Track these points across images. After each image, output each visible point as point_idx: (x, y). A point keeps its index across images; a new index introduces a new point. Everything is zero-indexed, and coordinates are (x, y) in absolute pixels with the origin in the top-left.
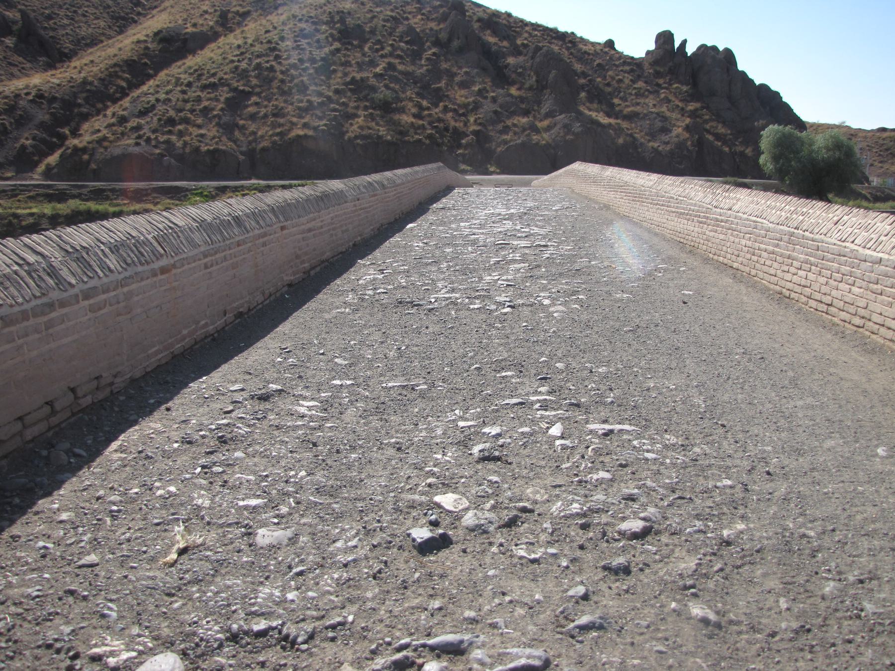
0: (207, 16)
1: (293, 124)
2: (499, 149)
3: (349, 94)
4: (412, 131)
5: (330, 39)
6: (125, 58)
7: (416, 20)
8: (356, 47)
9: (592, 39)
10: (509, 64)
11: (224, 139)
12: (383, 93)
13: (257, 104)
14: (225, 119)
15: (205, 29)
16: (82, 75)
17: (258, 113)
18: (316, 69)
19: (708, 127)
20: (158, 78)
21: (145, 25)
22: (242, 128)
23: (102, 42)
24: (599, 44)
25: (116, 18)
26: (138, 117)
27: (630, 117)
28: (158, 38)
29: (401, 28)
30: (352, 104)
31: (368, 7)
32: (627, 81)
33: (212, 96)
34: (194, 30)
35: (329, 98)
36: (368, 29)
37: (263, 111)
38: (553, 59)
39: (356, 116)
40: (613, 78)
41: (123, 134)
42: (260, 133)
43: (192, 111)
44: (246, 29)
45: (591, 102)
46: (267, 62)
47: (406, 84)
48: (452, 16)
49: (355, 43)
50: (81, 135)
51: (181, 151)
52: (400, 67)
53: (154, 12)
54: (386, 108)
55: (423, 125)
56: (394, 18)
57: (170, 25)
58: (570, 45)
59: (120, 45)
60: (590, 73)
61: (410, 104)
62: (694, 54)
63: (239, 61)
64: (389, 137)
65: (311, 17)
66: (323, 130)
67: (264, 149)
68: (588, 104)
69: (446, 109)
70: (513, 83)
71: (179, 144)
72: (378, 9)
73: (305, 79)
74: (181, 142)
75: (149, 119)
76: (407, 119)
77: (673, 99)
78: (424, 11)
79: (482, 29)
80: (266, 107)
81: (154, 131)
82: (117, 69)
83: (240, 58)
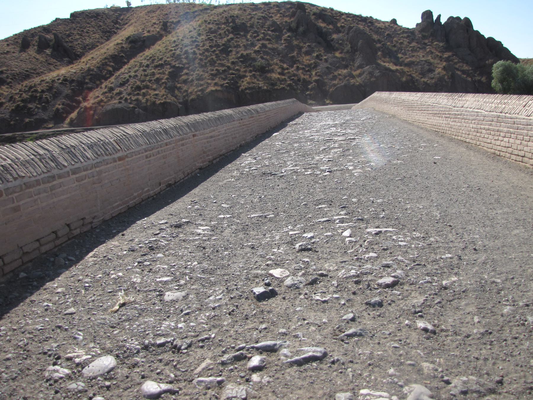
0: (155, 26)
1: (209, 84)
2: (331, 90)
3: (240, 64)
4: (278, 83)
5: (227, 33)
6: (111, 54)
7: (277, 17)
8: (242, 36)
9: (383, 20)
10: (334, 39)
11: (169, 96)
12: (260, 62)
13: (187, 74)
14: (169, 84)
15: (154, 33)
16: (88, 66)
17: (188, 79)
18: (220, 51)
19: (457, 66)
20: (129, 64)
22: (179, 89)
23: (98, 46)
24: (387, 22)
25: (104, 32)
26: (119, 87)
27: (410, 65)
29: (268, 23)
30: (242, 70)
31: (248, 12)
32: (405, 43)
33: (161, 71)
34: (149, 34)
35: (229, 67)
36: (248, 25)
38: (360, 33)
40: (397, 42)
41: (112, 97)
42: (190, 91)
43: (150, 81)
44: (178, 31)
45: (385, 57)
46: (192, 49)
47: (273, 55)
48: (298, 13)
49: (242, 33)
50: (88, 100)
51: (145, 105)
52: (269, 46)
53: (126, 26)
54: (263, 70)
55: (285, 79)
56: (264, 17)
57: (134, 33)
58: (370, 24)
59: (108, 47)
60: (383, 40)
61: (277, 67)
62: (445, 23)
63: (175, 50)
64: (265, 88)
65: (215, 21)
66: (226, 86)
67: (193, 100)
68: (383, 59)
69: (298, 68)
70: (337, 50)
71: (144, 101)
72: (254, 13)
73: (214, 57)
74: (145, 99)
75: (126, 88)
76: (275, 76)
77: (435, 51)
78: (281, 12)
79: (317, 19)
80: (192, 75)
81: (129, 94)
82: (107, 61)
83: (176, 48)
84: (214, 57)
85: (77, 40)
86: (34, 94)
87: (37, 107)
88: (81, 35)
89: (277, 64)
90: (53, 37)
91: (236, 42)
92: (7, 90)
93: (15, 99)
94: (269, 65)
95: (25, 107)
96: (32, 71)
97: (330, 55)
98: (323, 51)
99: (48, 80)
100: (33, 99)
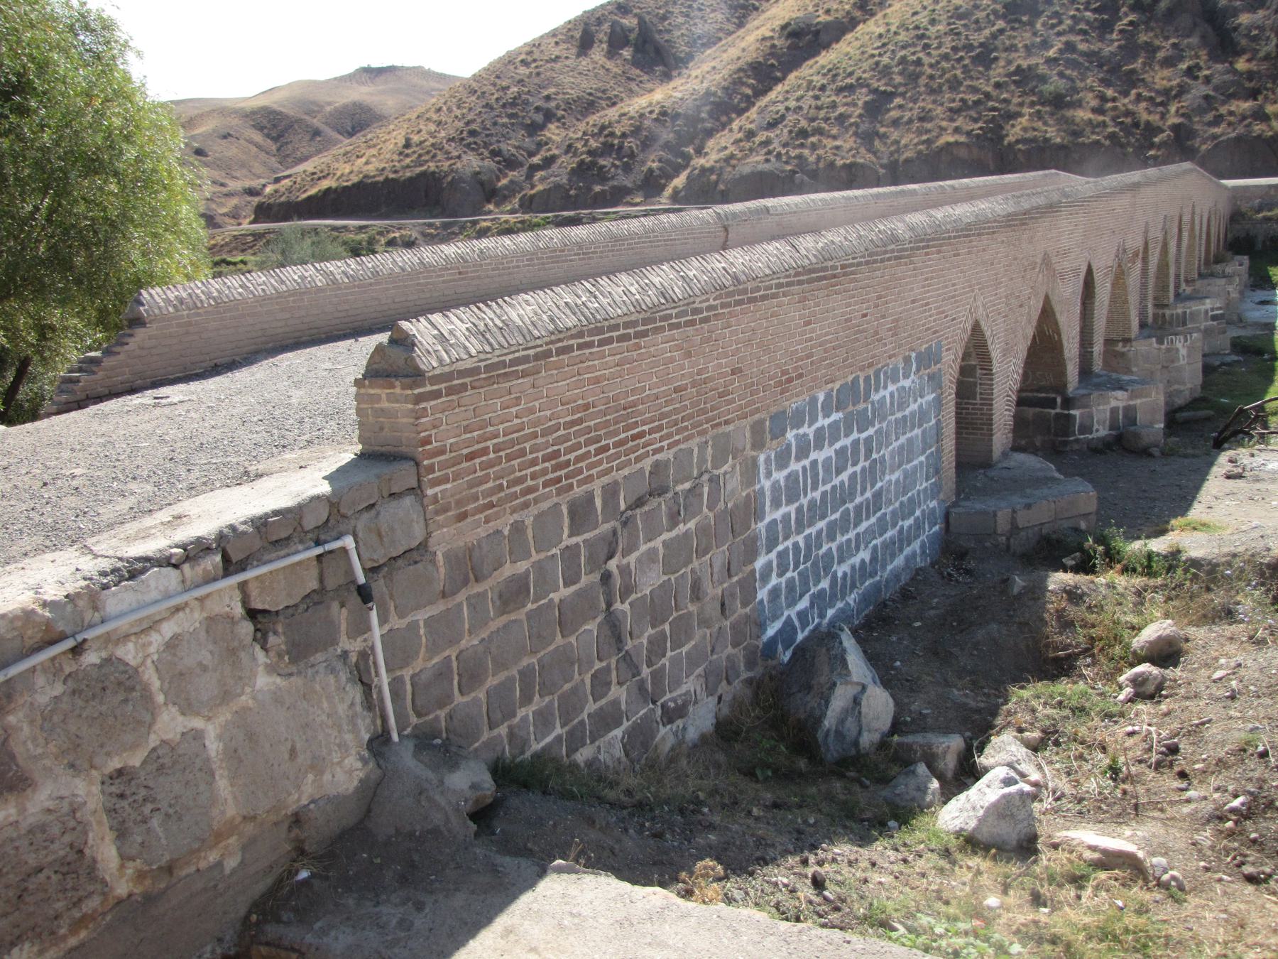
1: (942, 129)
2: (1204, 147)
3: (1013, 87)
4: (1088, 130)
5: (992, 17)
6: (750, 60)
8: (1025, 24)
11: (862, 150)
12: (1056, 83)
13: (900, 107)
14: (863, 127)
15: (839, 15)
16: (705, 85)
17: (902, 117)
20: (786, 82)
21: (768, 14)
22: (883, 137)
23: (720, 39)
28: (786, 32)
30: (1016, 100)
33: (849, 100)
34: (829, 18)
35: (988, 96)
37: (908, 115)
39: (1019, 115)
41: (751, 150)
42: (903, 142)
43: (826, 119)
44: (888, 11)
46: (914, 54)
47: (1087, 68)
49: (1025, 19)
50: (706, 154)
52: (1083, 47)
54: (1058, 102)
55: (1104, 122)
57: (798, 14)
59: (743, 45)
61: (1091, 95)
63: (880, 55)
64: (1058, 140)
66: (978, 136)
67: (907, 161)
70: (1238, 53)
71: (812, 159)
73: (958, 72)
76: (1082, 115)
80: (911, 109)
81: (785, 145)
84: (958, 72)
85: (678, 27)
86: (610, 139)
87: (614, 165)
88: (687, 16)
89: (1091, 89)
90: (635, 21)
91: (1010, 37)
92: (557, 131)
93: (576, 149)
94: (1075, 90)
95: (594, 164)
96: (600, 95)
97: (1219, 67)
98: (1205, 57)
99: (632, 113)
100: (607, 149)
